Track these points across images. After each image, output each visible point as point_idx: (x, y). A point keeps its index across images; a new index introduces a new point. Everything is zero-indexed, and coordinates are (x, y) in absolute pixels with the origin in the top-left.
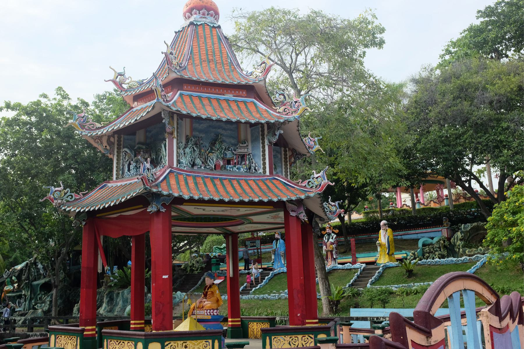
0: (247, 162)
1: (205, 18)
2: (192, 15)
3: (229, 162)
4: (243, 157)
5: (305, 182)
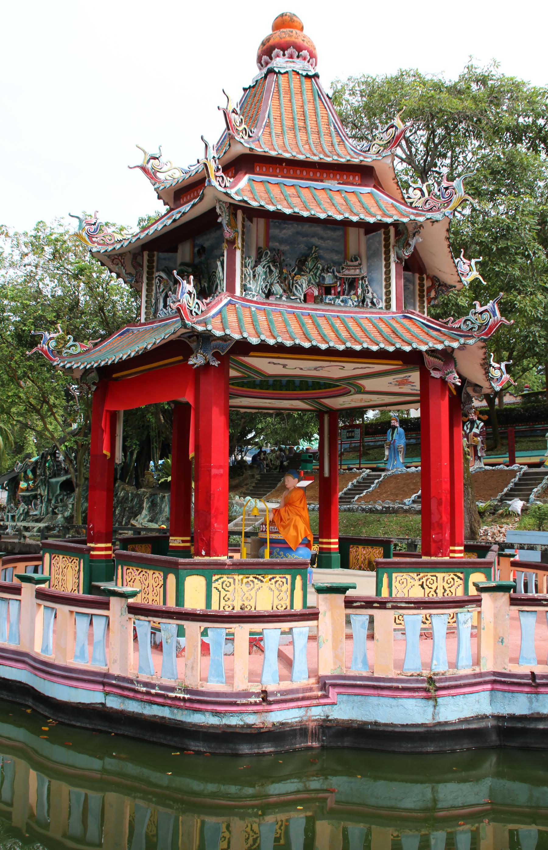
0: (360, 291)
1: (293, 62)
2: (271, 59)
3: (328, 290)
4: (352, 284)
5: (459, 322)
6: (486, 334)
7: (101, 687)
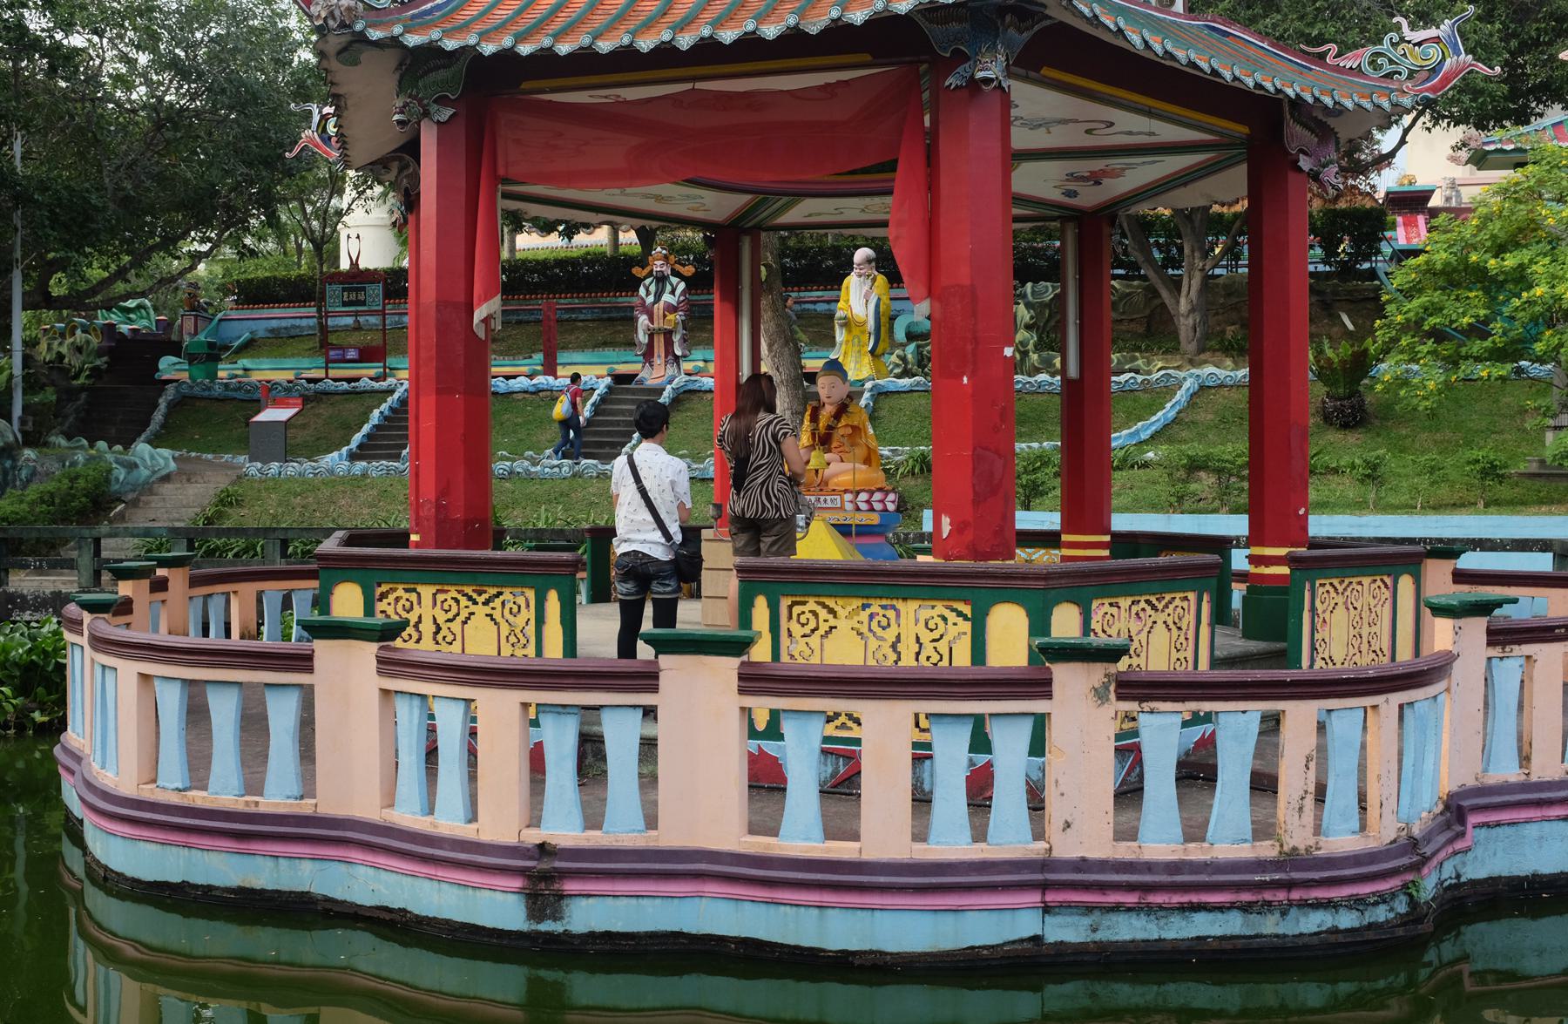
5: (1357, 56)
6: (1434, 89)
7: (1034, 898)
